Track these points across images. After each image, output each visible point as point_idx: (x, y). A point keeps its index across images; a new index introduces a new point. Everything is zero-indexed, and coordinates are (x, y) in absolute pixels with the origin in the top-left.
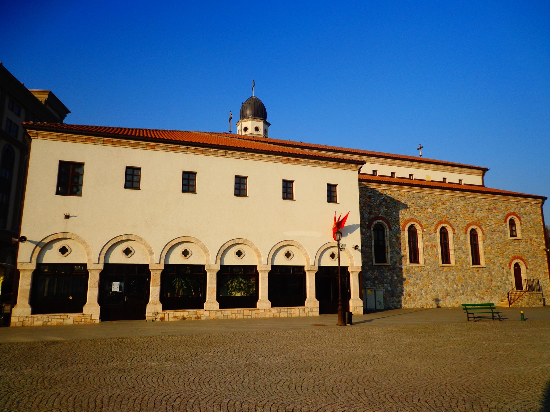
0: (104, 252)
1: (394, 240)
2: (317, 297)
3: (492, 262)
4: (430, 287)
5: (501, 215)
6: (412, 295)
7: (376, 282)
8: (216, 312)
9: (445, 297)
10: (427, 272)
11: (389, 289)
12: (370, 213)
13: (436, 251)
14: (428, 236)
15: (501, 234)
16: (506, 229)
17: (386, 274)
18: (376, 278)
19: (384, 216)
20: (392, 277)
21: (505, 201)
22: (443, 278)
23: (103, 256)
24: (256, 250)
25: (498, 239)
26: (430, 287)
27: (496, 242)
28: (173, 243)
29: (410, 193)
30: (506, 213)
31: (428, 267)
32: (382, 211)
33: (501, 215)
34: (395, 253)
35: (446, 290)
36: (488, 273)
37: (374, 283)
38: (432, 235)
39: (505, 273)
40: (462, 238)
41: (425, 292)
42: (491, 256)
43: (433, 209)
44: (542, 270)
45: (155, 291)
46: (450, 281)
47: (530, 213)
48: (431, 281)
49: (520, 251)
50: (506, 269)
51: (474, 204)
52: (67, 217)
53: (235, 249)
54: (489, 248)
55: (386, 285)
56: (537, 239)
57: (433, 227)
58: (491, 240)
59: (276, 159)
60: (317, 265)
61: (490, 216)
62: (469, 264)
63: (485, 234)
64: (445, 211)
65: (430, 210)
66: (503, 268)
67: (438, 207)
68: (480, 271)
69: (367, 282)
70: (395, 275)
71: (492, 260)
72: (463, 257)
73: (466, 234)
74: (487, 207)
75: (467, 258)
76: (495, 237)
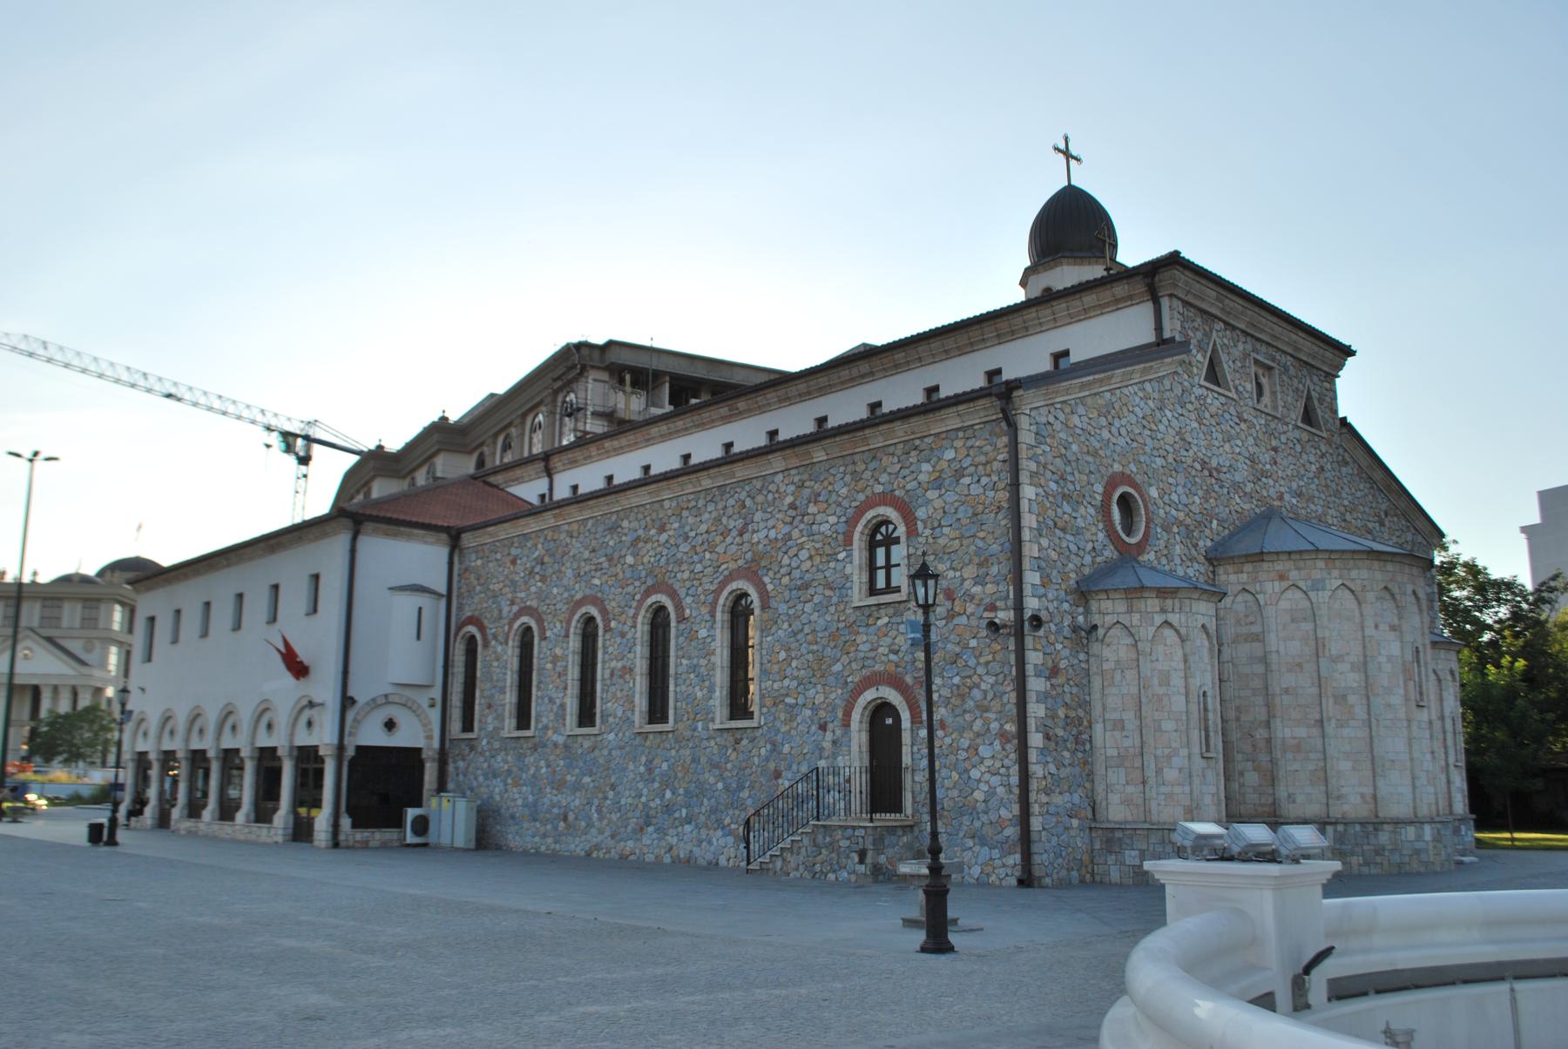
1: (549, 666)
3: (786, 704)
5: (833, 519)
6: (571, 817)
7: (509, 781)
9: (642, 829)
10: (605, 752)
11: (531, 798)
12: (512, 603)
13: (631, 685)
14: (618, 640)
15: (828, 593)
17: (527, 760)
18: (509, 772)
20: (538, 768)
21: (857, 458)
22: (642, 769)
25: (814, 617)
27: (807, 630)
30: (854, 504)
31: (611, 736)
33: (833, 519)
34: (546, 700)
35: (645, 805)
36: (769, 747)
37: (506, 784)
38: (629, 636)
39: (827, 745)
40: (703, 633)
41: (599, 811)
42: (786, 682)
43: (635, 555)
44: (994, 726)
46: (657, 778)
47: (959, 474)
48: (613, 780)
49: (896, 652)
50: (835, 730)
51: (748, 502)
54: (783, 655)
55: (524, 788)
56: (984, 584)
57: (631, 612)
58: (790, 626)
60: (287, 745)
61: (795, 534)
62: (713, 720)
63: (773, 604)
64: (665, 552)
65: (630, 560)
66: (823, 727)
67: (649, 546)
68: (745, 742)
69: (494, 781)
70: (542, 763)
71: (789, 700)
72: (699, 694)
74: (789, 499)
75: (711, 698)
76: (808, 608)
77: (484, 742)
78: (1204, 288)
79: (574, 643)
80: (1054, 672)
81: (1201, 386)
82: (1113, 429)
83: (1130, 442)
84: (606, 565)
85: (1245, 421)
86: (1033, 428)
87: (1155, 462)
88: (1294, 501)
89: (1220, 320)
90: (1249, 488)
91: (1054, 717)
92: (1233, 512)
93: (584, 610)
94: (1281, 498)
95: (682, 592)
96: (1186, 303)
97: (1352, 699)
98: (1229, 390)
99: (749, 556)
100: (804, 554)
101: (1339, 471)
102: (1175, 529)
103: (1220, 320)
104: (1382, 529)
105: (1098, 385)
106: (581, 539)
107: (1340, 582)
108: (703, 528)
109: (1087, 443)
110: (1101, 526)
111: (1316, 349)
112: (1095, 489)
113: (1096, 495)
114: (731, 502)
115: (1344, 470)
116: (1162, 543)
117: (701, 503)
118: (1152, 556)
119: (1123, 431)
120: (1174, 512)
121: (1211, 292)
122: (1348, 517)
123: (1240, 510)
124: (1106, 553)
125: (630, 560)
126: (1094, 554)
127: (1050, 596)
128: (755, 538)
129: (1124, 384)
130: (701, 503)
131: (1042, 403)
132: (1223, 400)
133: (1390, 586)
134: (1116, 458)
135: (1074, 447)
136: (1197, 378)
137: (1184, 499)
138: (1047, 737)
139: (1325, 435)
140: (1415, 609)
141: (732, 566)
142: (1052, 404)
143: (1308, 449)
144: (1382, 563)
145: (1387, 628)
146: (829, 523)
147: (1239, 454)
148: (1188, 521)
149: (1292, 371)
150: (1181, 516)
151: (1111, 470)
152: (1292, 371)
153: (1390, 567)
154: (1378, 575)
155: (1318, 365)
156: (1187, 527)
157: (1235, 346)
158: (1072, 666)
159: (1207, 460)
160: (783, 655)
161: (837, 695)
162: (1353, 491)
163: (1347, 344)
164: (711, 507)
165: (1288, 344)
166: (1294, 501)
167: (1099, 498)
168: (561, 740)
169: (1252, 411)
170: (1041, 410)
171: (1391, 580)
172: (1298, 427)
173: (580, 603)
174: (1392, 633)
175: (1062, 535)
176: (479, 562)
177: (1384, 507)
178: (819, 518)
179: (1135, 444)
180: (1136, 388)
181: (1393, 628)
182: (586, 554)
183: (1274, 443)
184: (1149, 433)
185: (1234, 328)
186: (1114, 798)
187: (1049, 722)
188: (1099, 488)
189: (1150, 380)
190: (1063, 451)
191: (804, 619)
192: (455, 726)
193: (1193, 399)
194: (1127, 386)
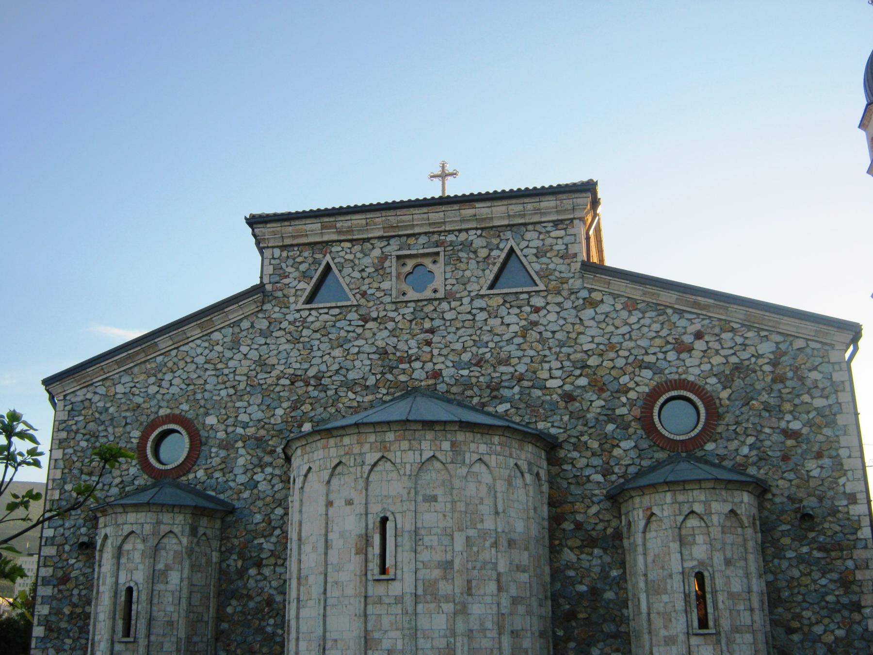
78: (300, 227)
80: (65, 579)
81: (298, 311)
82: (164, 383)
83: (183, 386)
85: (375, 319)
86: (69, 407)
87: (219, 395)
88: (465, 372)
89: (341, 241)
90: (371, 381)
91: (58, 612)
92: (343, 410)
94: (437, 375)
96: (283, 248)
97: (311, 579)
98: (349, 300)
101: (577, 316)
102: (240, 444)
103: (341, 241)
104: (684, 356)
105: (143, 355)
107: (306, 467)
109: (128, 402)
110: (134, 462)
111: (520, 207)
112: (131, 435)
113: (133, 440)
115: (588, 313)
116: (216, 461)
118: (200, 474)
119: (176, 381)
120: (239, 430)
121: (314, 226)
122: (593, 361)
123: (355, 404)
124: (137, 483)
126: (120, 486)
127: (67, 525)
129: (181, 343)
131: (78, 387)
132: (337, 311)
133: (344, 461)
134: (164, 404)
135: (111, 410)
136: (293, 307)
137: (260, 415)
138: (49, 629)
139: (542, 287)
140: (394, 475)
142: (92, 384)
143: (503, 311)
144: (339, 438)
145: (343, 503)
147: (359, 353)
148: (262, 432)
149: (478, 242)
150: (251, 431)
151: (152, 417)
152: (478, 242)
153: (347, 440)
154: (333, 452)
155: (536, 219)
156: (257, 439)
157: (366, 255)
158: (84, 574)
159: (299, 373)
162: (610, 328)
163: (585, 179)
165: (463, 221)
166: (465, 372)
167: (135, 441)
169: (389, 307)
170: (78, 393)
171: (346, 454)
172: (483, 296)
174: (348, 507)
175: (87, 478)
177: (697, 327)
179: (192, 387)
180: (199, 342)
181: (349, 502)
183: (427, 325)
184: (213, 373)
185: (368, 240)
187: (53, 618)
188: (136, 434)
189: (219, 330)
190: (97, 415)
193: (285, 325)
194: (187, 343)
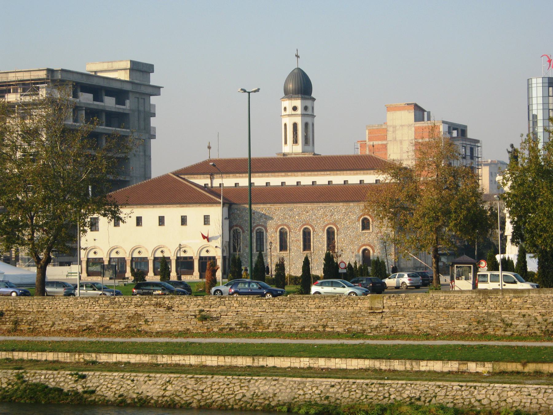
0: (109, 253)
2: (199, 271)
4: (293, 265)
8: (152, 277)
16: (358, 226)
19: (263, 224)
23: (108, 255)
24: (169, 250)
26: (293, 265)
28: (134, 248)
29: (282, 208)
32: (262, 220)
40: (320, 234)
42: (344, 245)
45: (128, 269)
51: (332, 210)
52: (95, 240)
53: (160, 250)
57: (298, 228)
59: (177, 206)
60: (198, 256)
61: (345, 218)
65: (297, 217)
66: (353, 253)
73: (324, 231)
74: (344, 211)
76: (349, 232)
77: (245, 254)
79: (278, 234)
84: (289, 218)
93: (282, 227)
95: (314, 226)
99: (333, 221)
100: (347, 222)
106: (280, 211)
108: (320, 213)
114: (328, 209)
117: (319, 209)
125: (297, 217)
128: (335, 217)
130: (319, 209)
141: (329, 222)
146: (354, 217)
160: (342, 240)
161: (356, 247)
164: (322, 210)
168: (275, 254)
173: (280, 225)
176: (238, 212)
178: (351, 216)
182: (282, 215)
186: (402, 264)
191: (348, 233)
192: (232, 251)
